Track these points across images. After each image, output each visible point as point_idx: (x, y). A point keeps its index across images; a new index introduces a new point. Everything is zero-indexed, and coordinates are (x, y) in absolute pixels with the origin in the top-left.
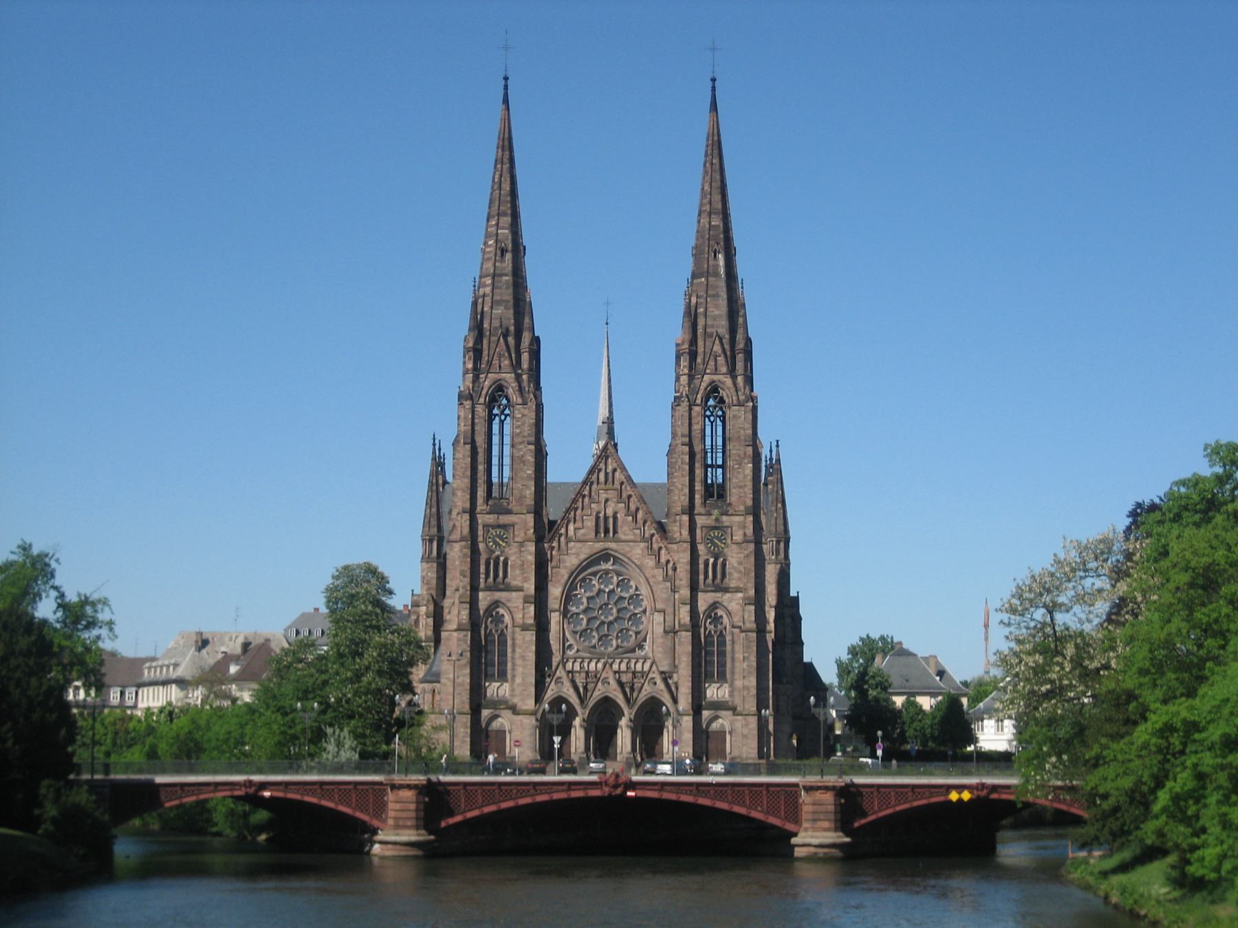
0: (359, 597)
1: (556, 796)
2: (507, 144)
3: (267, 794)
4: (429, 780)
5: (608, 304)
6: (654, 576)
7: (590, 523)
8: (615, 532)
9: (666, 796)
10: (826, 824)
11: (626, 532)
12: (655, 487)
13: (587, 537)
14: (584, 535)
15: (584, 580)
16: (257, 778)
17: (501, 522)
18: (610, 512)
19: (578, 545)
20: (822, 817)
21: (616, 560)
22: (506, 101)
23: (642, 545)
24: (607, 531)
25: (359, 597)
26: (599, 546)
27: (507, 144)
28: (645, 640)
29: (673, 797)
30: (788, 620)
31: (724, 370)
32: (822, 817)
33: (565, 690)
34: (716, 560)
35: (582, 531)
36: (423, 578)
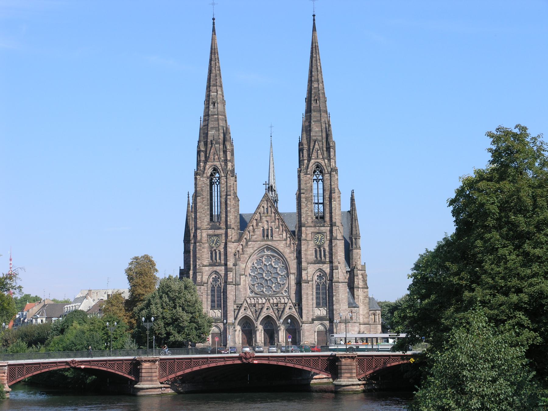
1: (219, 364)
2: (214, 51)
3: (83, 367)
5: (271, 127)
6: (290, 257)
7: (259, 232)
8: (272, 237)
9: (272, 363)
11: (276, 237)
12: (290, 215)
13: (258, 239)
14: (256, 238)
16: (77, 359)
17: (216, 233)
19: (253, 243)
20: (347, 371)
22: (214, 30)
23: (284, 242)
24: (267, 236)
27: (214, 51)
29: (275, 363)
30: (360, 277)
31: (321, 157)
32: (347, 371)
33: (248, 313)
34: (320, 248)
35: (255, 236)
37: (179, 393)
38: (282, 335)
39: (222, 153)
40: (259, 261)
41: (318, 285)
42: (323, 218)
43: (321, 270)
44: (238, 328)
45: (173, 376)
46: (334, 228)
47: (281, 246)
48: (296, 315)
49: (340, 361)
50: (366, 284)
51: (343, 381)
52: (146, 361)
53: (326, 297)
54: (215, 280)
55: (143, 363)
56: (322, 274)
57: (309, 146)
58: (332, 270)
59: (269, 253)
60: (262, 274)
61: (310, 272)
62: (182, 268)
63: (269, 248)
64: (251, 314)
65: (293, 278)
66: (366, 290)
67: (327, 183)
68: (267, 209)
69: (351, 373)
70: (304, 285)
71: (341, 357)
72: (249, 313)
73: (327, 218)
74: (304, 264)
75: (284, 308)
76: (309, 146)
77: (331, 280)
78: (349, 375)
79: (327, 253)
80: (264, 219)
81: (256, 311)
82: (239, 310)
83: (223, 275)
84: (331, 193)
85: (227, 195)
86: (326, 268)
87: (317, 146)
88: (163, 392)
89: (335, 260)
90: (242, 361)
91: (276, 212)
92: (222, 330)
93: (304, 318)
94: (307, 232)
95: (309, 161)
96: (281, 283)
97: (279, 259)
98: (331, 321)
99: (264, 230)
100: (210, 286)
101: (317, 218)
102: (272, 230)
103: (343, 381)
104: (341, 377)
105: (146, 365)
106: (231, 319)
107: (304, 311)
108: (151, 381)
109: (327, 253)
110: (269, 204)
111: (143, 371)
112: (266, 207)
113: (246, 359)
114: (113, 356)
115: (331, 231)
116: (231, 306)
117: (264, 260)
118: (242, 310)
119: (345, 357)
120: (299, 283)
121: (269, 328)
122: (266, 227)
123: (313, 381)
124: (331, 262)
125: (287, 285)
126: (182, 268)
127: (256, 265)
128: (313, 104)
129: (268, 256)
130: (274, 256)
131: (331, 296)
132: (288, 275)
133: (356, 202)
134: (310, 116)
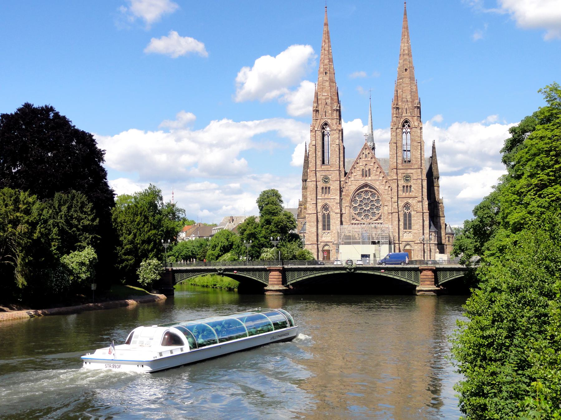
0: (270, 202)
4: (283, 267)
7: (360, 173)
10: (429, 283)
15: (358, 194)
18: (367, 169)
21: (371, 187)
25: (270, 202)
26: (363, 182)
28: (381, 216)
32: (427, 280)
36: (303, 195)
47: (377, 185)
62: (301, 200)
63: (366, 185)
97: (375, 194)
126: (301, 200)
129: (366, 191)
130: (371, 192)
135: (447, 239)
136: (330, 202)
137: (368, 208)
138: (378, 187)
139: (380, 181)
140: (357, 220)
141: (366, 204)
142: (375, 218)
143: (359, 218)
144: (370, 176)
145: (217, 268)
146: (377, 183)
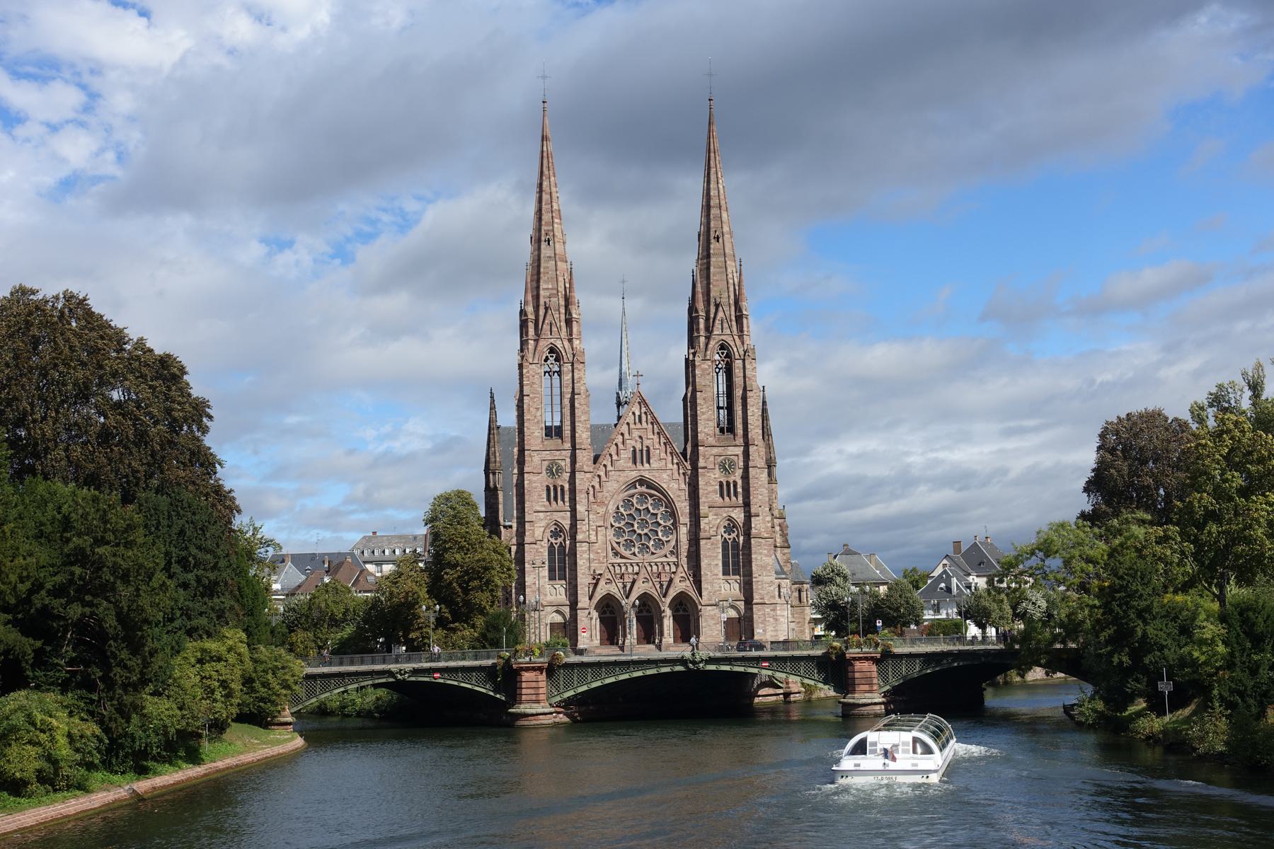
1: (649, 672)
7: (626, 455)
21: (650, 486)
26: (634, 475)
29: (741, 669)
30: (777, 528)
37: (574, 720)
38: (668, 623)
39: (563, 324)
40: (628, 503)
41: (725, 542)
42: (731, 429)
43: (730, 519)
44: (595, 614)
45: (571, 693)
46: (752, 449)
48: (693, 593)
49: (852, 665)
50: (787, 541)
51: (859, 697)
52: (527, 669)
53: (738, 560)
54: (555, 534)
55: (524, 673)
56: (731, 526)
57: (708, 312)
58: (748, 517)
59: (644, 489)
60: (632, 525)
61: (712, 523)
63: (642, 481)
64: (616, 591)
65: (683, 531)
66: (786, 551)
67: (738, 372)
68: (640, 416)
69: (871, 684)
70: (702, 542)
71: (854, 659)
72: (615, 589)
73: (740, 431)
74: (703, 509)
75: (671, 581)
76: (708, 312)
77: (748, 535)
78: (866, 687)
79: (740, 490)
80: (636, 434)
81: (625, 587)
82: (596, 585)
83: (567, 527)
84: (745, 389)
85: (573, 393)
86: (739, 515)
87: (721, 314)
88: (557, 720)
89: (753, 500)
90: (687, 667)
91: (655, 422)
92: (568, 616)
93: (704, 600)
94: (707, 457)
95: (708, 338)
96: (664, 539)
97: (660, 500)
98: (749, 601)
99: (634, 451)
100: (545, 544)
101: (722, 430)
102: (648, 451)
103: (859, 697)
104: (854, 691)
105: (526, 676)
106: (583, 601)
107: (704, 585)
108: (538, 701)
109: (740, 490)
110: (644, 409)
111: (524, 685)
112: (637, 413)
113: (694, 663)
114: (470, 659)
115: (746, 455)
116: (584, 580)
117: (635, 501)
118: (602, 583)
119: (860, 659)
120: (695, 540)
121: (608, 615)
122: (638, 447)
123: (757, 700)
124: (747, 505)
125: (673, 543)
127: (622, 510)
128: (714, 246)
129: (641, 494)
130: (651, 496)
131: (749, 562)
132: (675, 525)
133: (769, 407)
134: (708, 264)
135: (796, 594)
136: (563, 518)
137: (646, 531)
138: (665, 486)
139: (669, 472)
140: (622, 557)
141: (644, 523)
142: (663, 552)
143: (627, 553)
144: (648, 462)
145: (393, 667)
146: (665, 476)
